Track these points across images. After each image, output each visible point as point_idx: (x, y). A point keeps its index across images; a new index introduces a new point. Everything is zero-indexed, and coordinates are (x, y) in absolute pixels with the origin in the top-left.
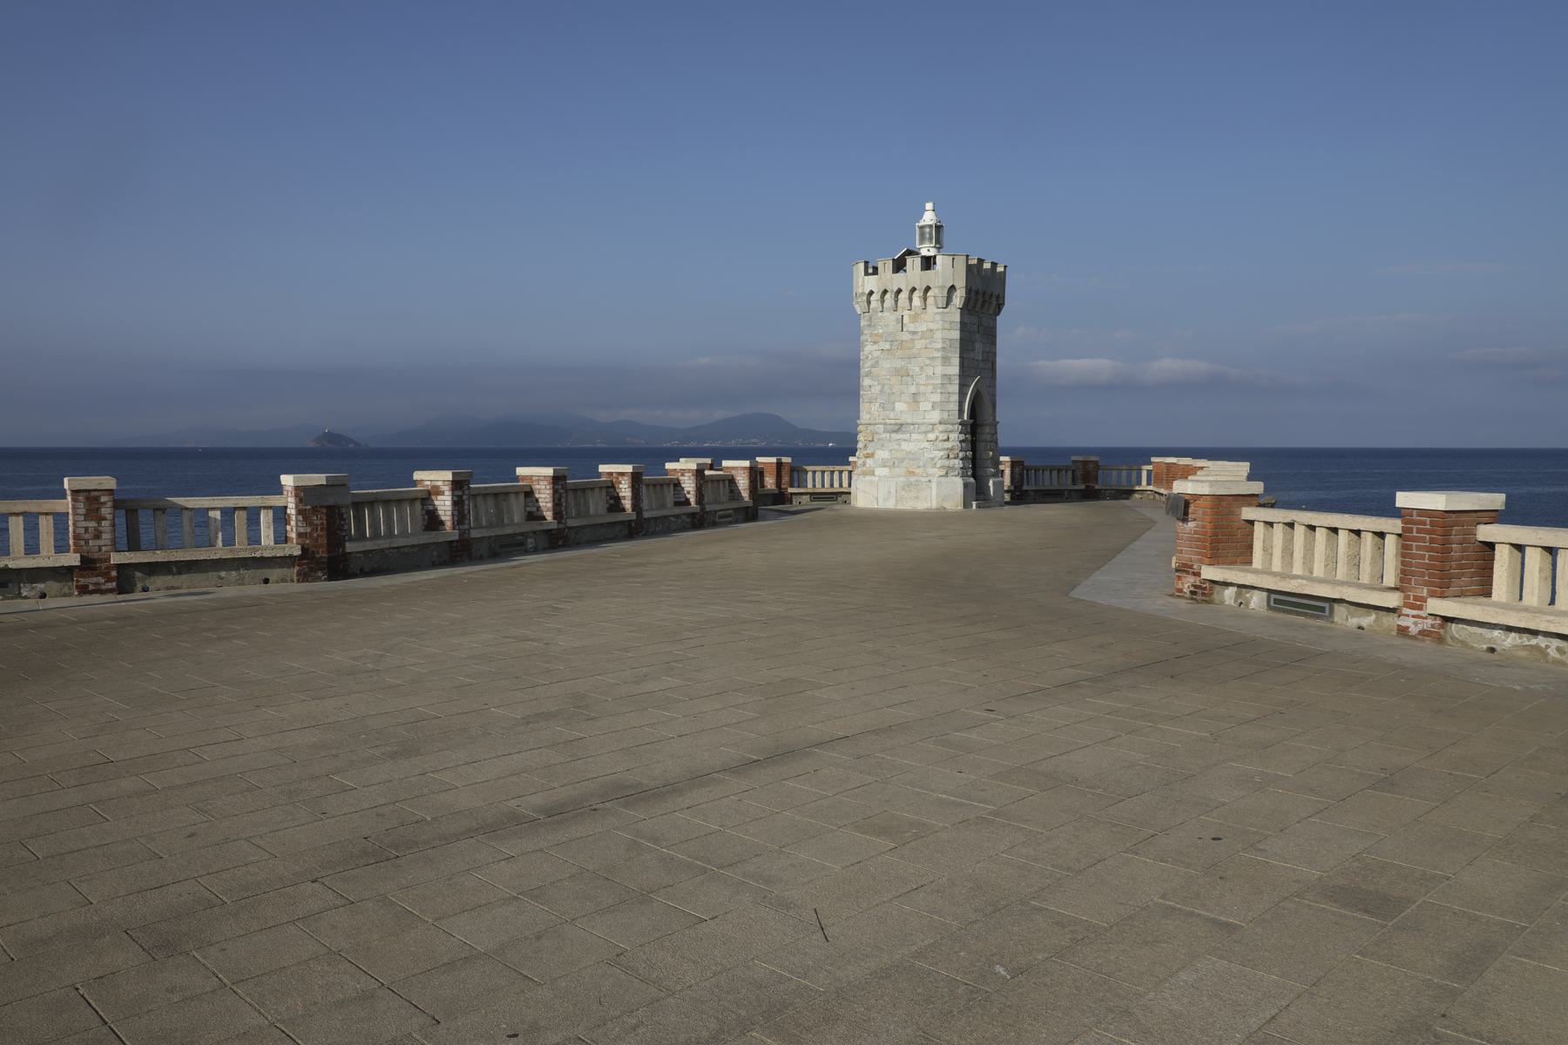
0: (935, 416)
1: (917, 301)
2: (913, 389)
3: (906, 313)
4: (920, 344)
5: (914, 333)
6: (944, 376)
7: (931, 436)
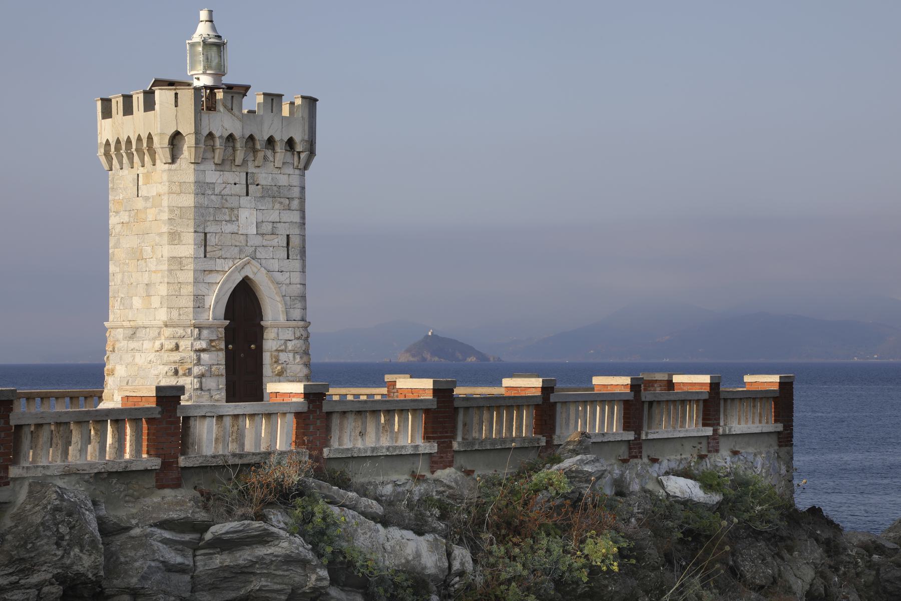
0: (162, 315)
2: (146, 278)
3: (141, 171)
4: (151, 214)
5: (147, 199)
6: (172, 259)
7: (157, 344)
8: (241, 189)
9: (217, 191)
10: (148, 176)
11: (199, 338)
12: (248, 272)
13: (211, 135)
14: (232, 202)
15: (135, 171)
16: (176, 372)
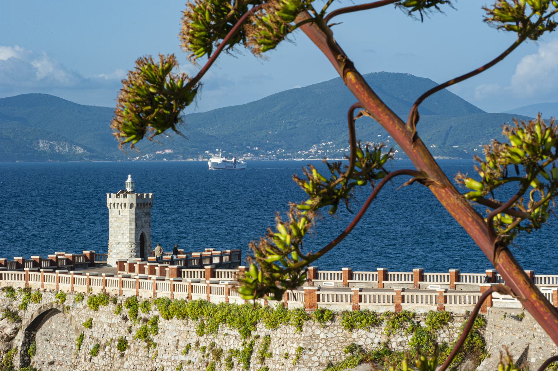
1: (123, 207)
2: (122, 232)
3: (120, 210)
4: (124, 219)
10: (123, 211)
15: (118, 210)
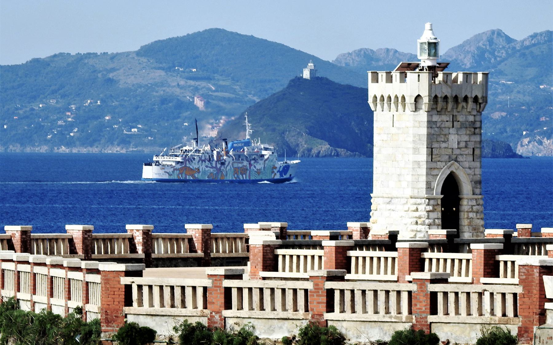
0: (409, 192)
8: (450, 124)
9: (438, 125)
11: (428, 205)
12: (453, 169)
13: (436, 97)
14: (446, 131)
16: (417, 223)
